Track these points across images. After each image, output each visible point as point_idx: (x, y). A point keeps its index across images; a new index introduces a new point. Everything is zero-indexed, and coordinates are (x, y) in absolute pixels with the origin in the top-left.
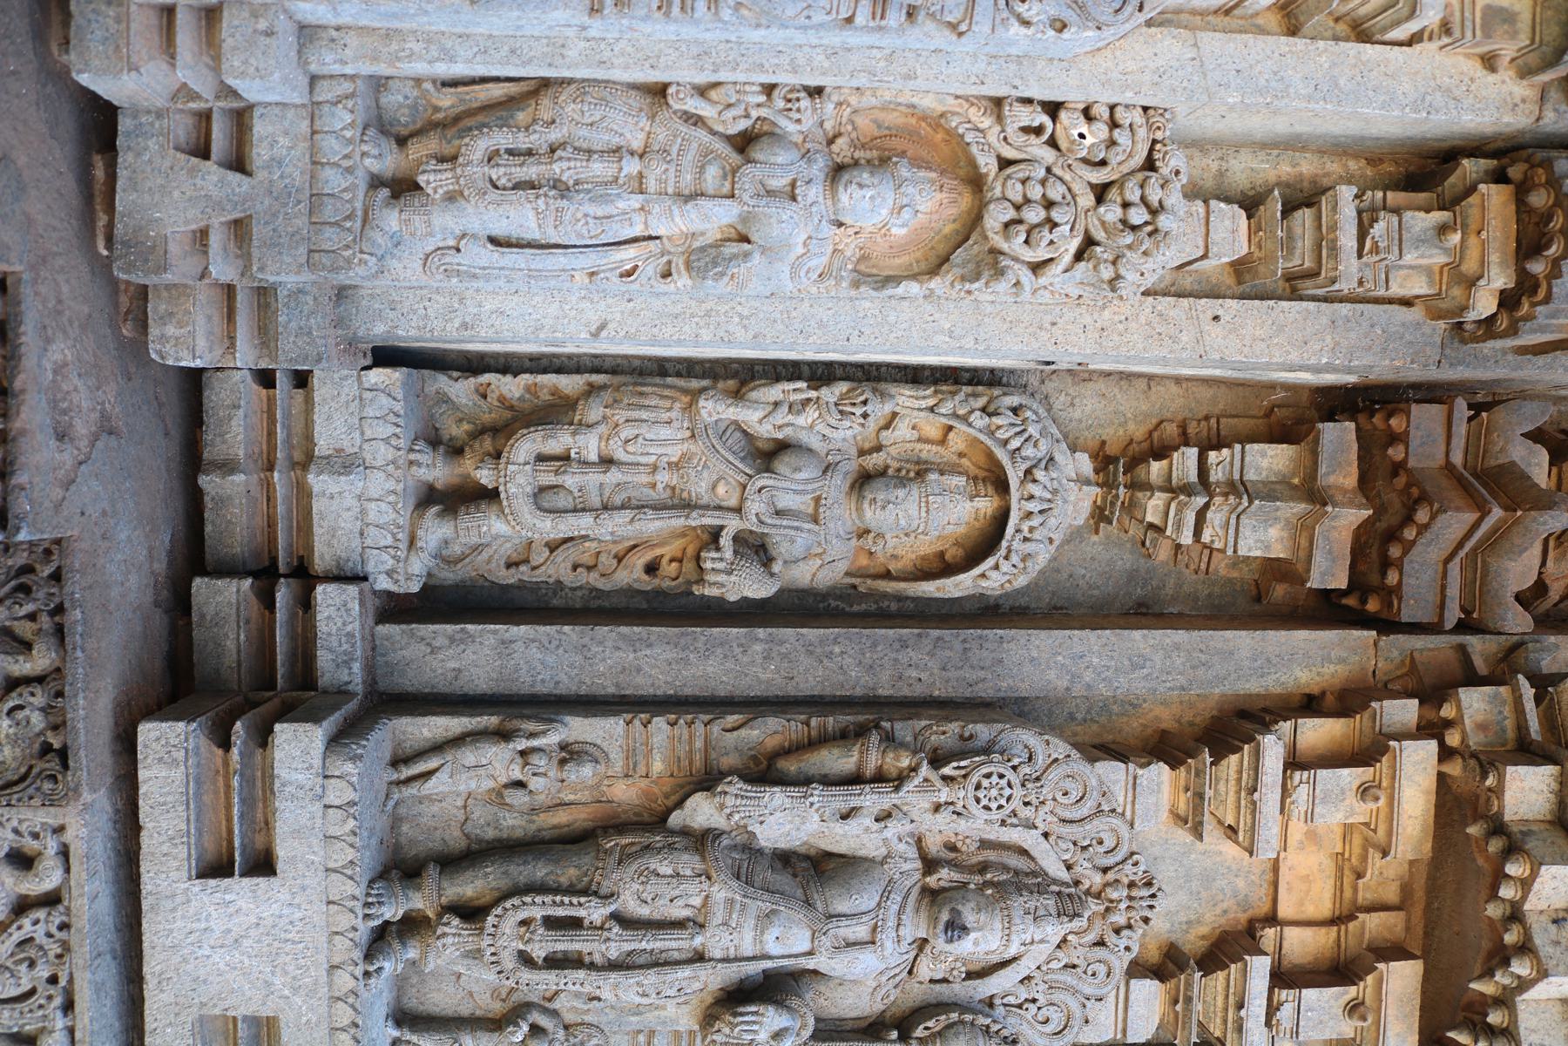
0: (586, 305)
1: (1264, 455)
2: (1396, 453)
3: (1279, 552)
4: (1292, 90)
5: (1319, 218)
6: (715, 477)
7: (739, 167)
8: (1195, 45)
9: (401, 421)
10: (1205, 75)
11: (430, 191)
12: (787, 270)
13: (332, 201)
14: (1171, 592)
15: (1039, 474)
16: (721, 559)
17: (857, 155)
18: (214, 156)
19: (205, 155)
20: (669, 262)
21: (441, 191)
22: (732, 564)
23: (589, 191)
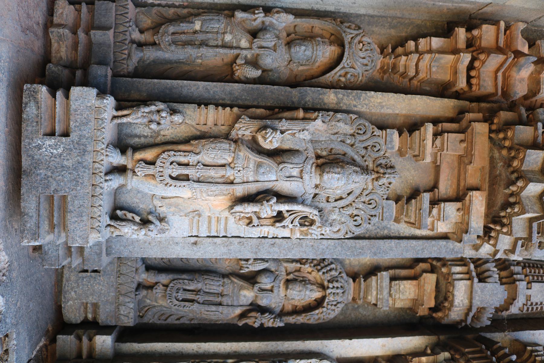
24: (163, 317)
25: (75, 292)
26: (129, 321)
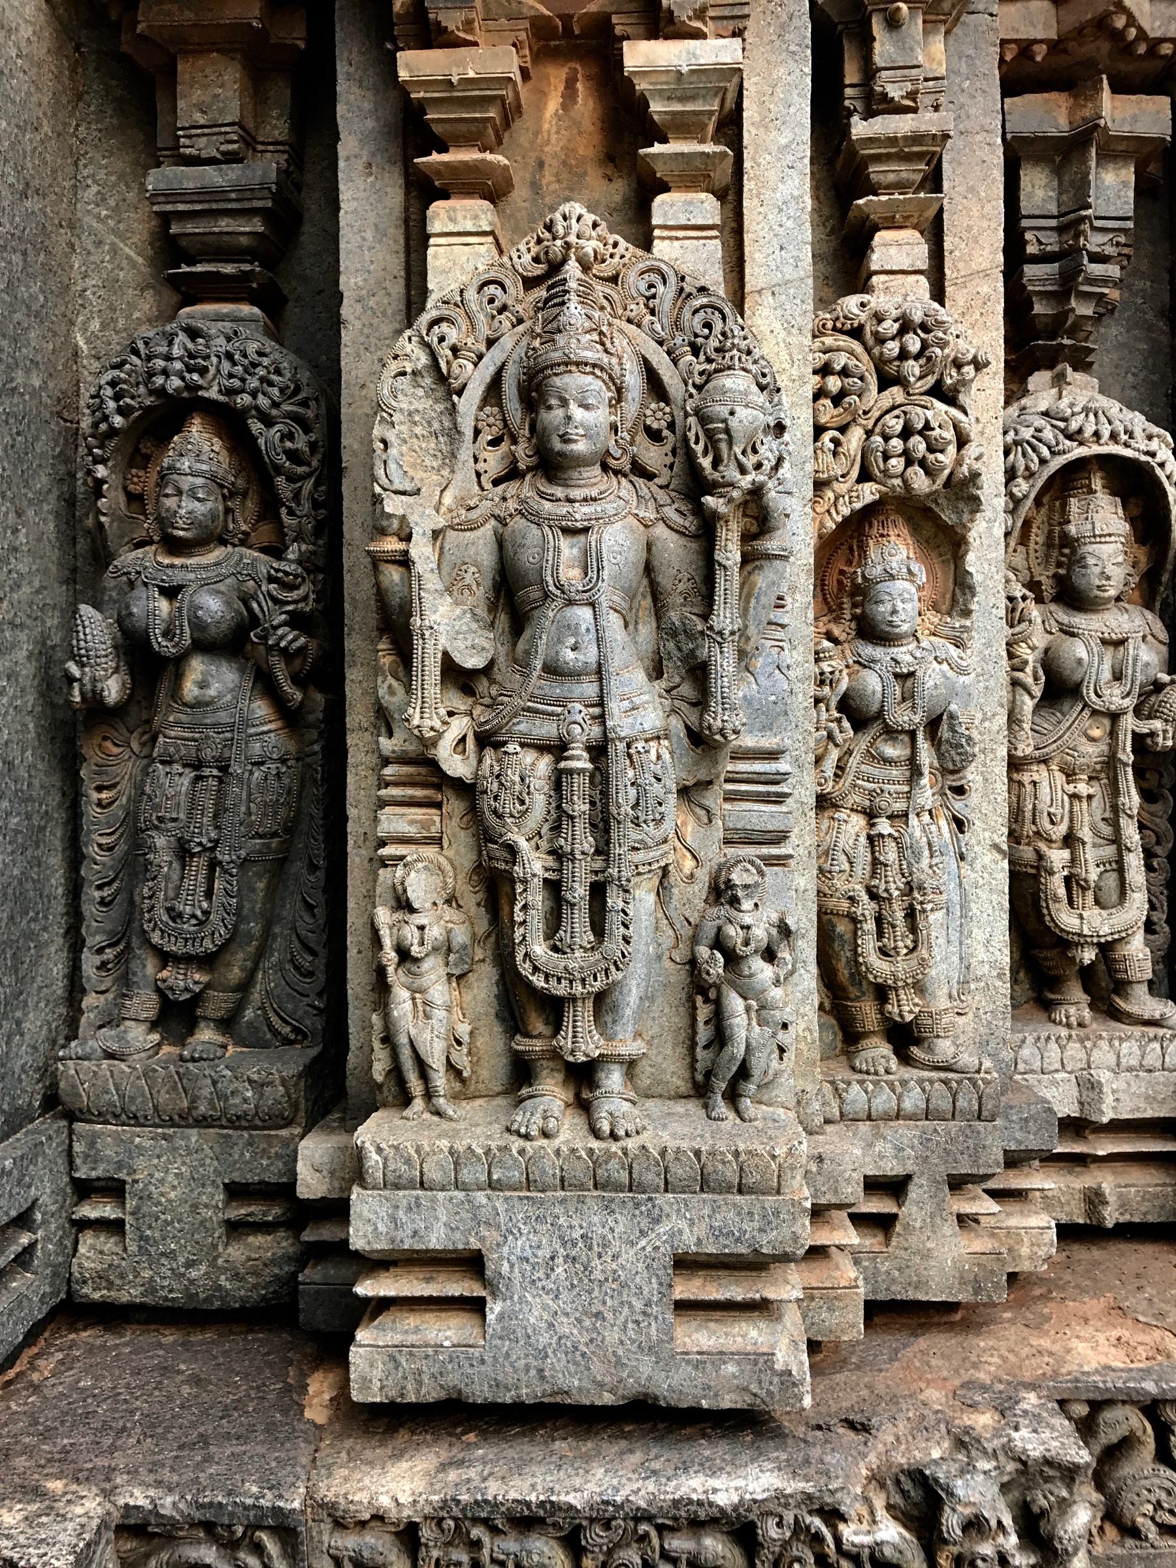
0: (978, 865)
1: (1031, 195)
2: (1040, 53)
3: (1128, 174)
4: (796, 193)
5: (878, 158)
6: (1084, 740)
7: (887, 725)
8: (759, 292)
9: (1044, 1035)
10: (787, 282)
11: (917, 1010)
12: (962, 679)
13: (933, 1101)
14: (1148, 283)
15: (1074, 425)
16: (1165, 731)
17: (848, 617)
18: (894, 1210)
19: (894, 1217)
20: (950, 788)
21: (917, 1000)
22: (1166, 721)
23: (909, 864)
24: (306, 960)
25: (190, 1264)
26: (278, 1082)
